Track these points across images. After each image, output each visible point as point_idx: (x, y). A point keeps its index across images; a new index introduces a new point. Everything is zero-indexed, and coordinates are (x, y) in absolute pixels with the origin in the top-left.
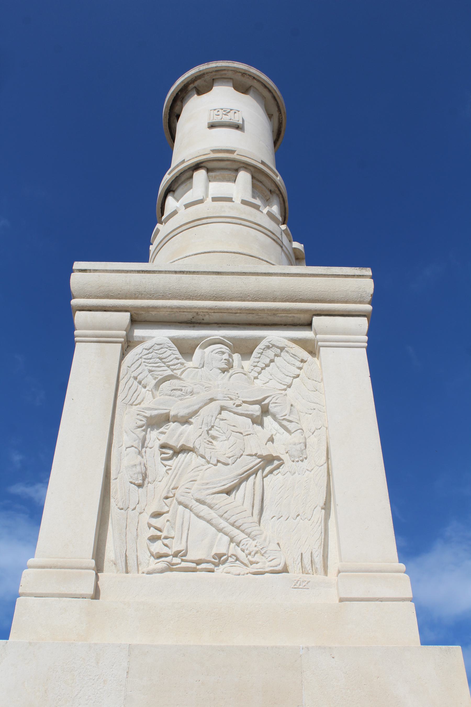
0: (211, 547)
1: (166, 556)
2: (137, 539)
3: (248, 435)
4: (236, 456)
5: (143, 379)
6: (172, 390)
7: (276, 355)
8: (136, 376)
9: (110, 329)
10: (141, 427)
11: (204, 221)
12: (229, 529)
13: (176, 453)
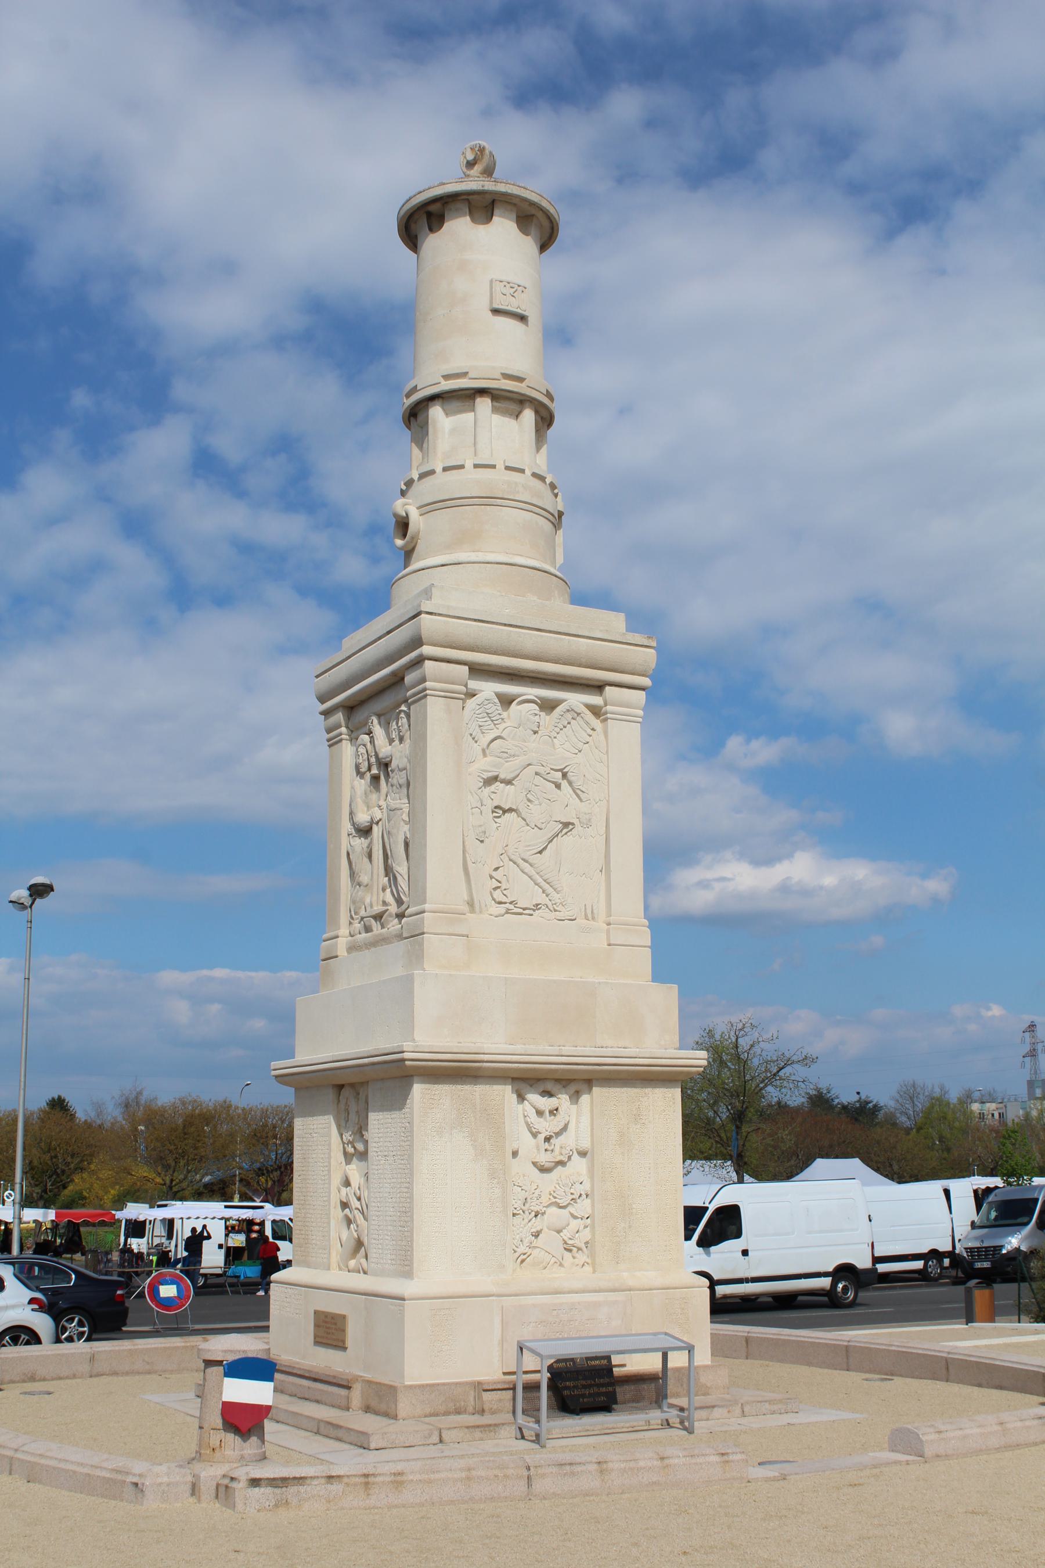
1: (505, 903)
7: (573, 718)
9: (453, 683)
11: (499, 502)
12: (543, 884)
13: (505, 811)
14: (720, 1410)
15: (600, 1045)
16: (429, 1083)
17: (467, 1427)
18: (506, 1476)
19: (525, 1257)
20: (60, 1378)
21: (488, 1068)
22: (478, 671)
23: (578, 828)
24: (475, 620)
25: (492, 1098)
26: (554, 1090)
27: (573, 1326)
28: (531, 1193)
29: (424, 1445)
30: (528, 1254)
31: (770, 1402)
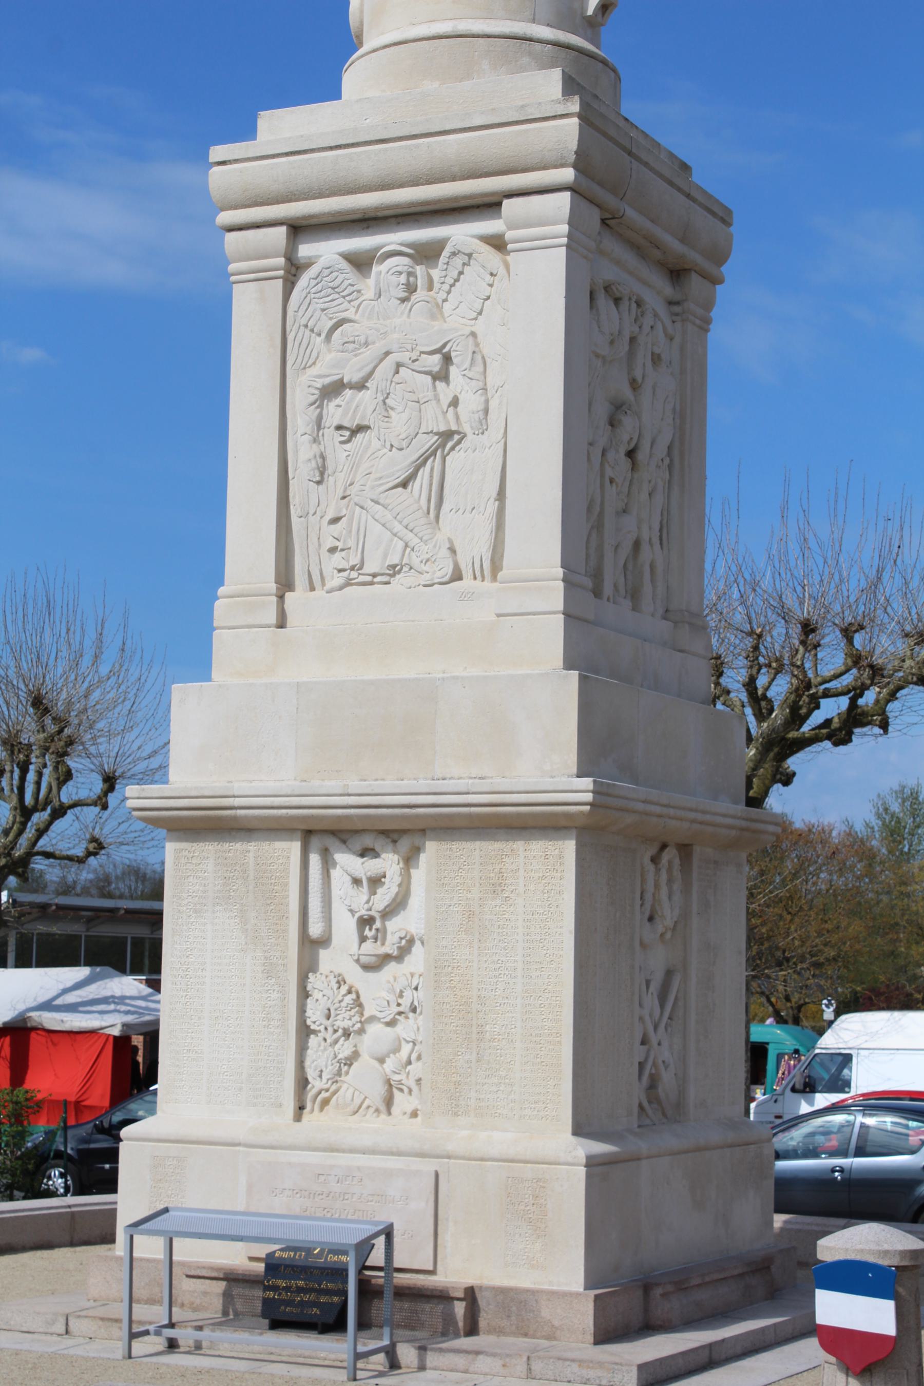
0: (385, 556)
2: (320, 549)
3: (425, 402)
4: (410, 437)
5: (315, 326)
6: (343, 344)
8: (305, 323)
10: (314, 403)
14: (489, 1360)
15: (440, 776)
16: (187, 841)
17: (102, 1319)
19: (326, 1095)
21: (246, 817)
23: (470, 436)
24: (287, 154)
25: (272, 861)
26: (378, 849)
27: (349, 1202)
28: (336, 1001)
29: (46, 1333)
30: (331, 1090)
31: (581, 1362)
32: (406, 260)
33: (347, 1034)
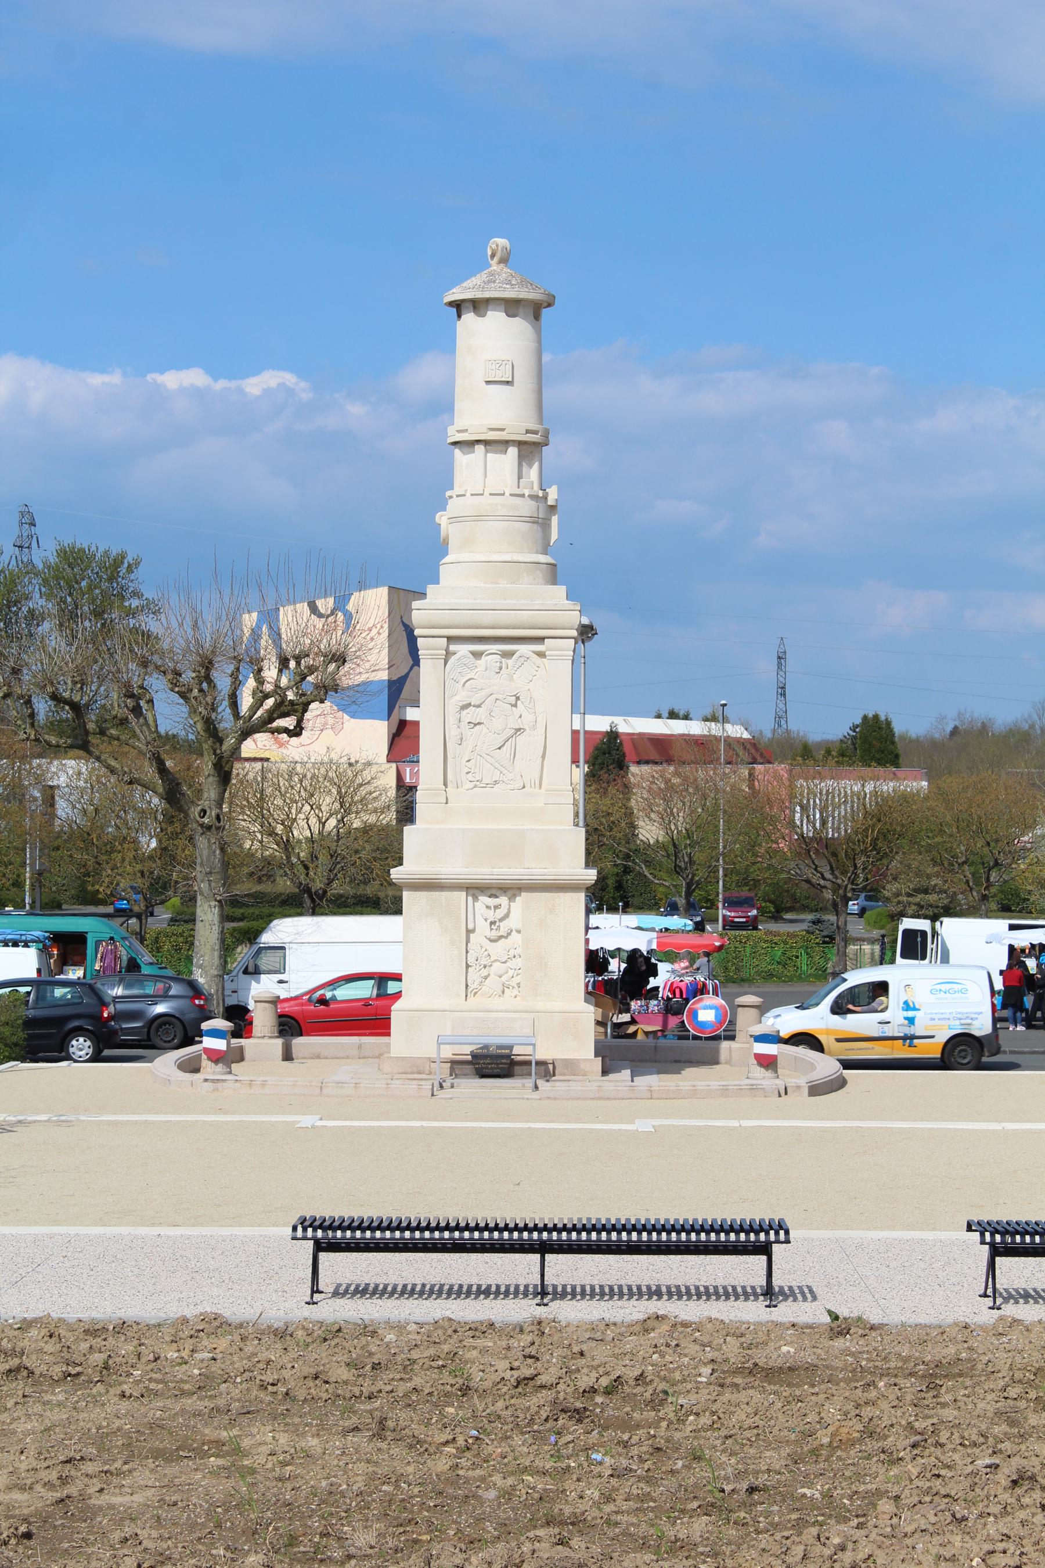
13: (475, 725)
18: (311, 1086)
20: (338, 1058)
22: (450, 639)
32: (499, 657)
33: (485, 967)
